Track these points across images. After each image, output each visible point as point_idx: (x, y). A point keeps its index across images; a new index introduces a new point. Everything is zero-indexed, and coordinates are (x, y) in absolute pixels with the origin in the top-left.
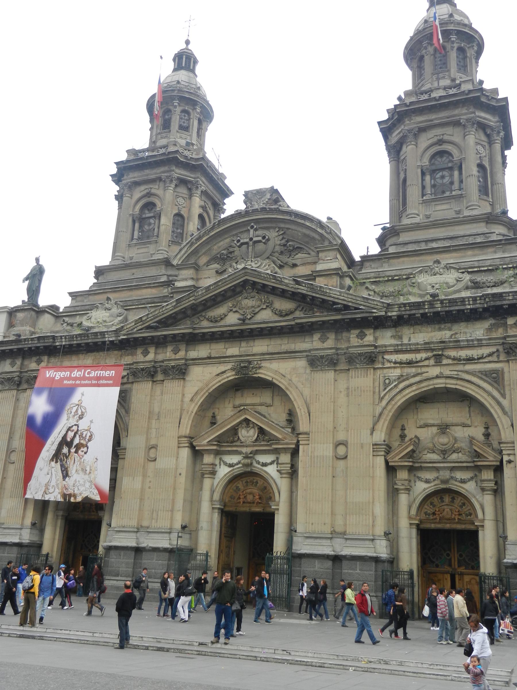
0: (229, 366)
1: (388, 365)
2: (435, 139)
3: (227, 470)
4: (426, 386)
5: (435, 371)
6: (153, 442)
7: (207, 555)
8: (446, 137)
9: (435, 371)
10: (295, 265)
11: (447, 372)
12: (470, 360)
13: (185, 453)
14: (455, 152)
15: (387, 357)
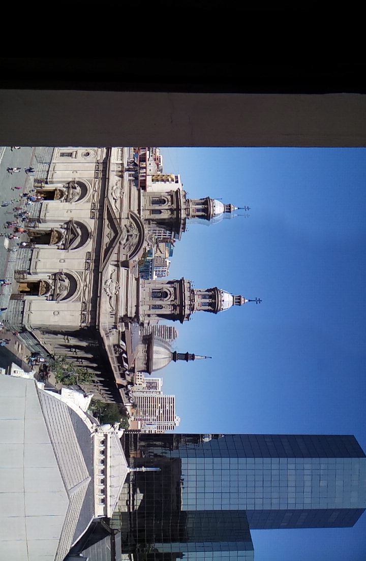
0: (93, 230)
1: (86, 273)
2: (172, 293)
3: (63, 232)
4: (78, 283)
5: (82, 285)
6: (73, 211)
7: (38, 227)
8: (172, 296)
9: (82, 285)
10: (124, 248)
11: (82, 288)
12: (84, 293)
13: (68, 219)
14: (166, 299)
15: (89, 273)
